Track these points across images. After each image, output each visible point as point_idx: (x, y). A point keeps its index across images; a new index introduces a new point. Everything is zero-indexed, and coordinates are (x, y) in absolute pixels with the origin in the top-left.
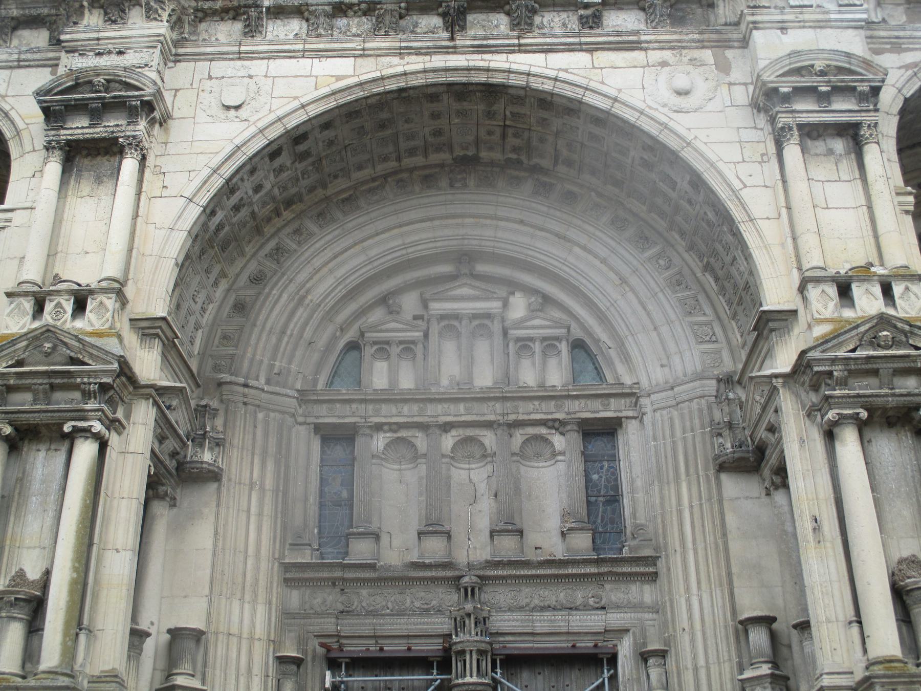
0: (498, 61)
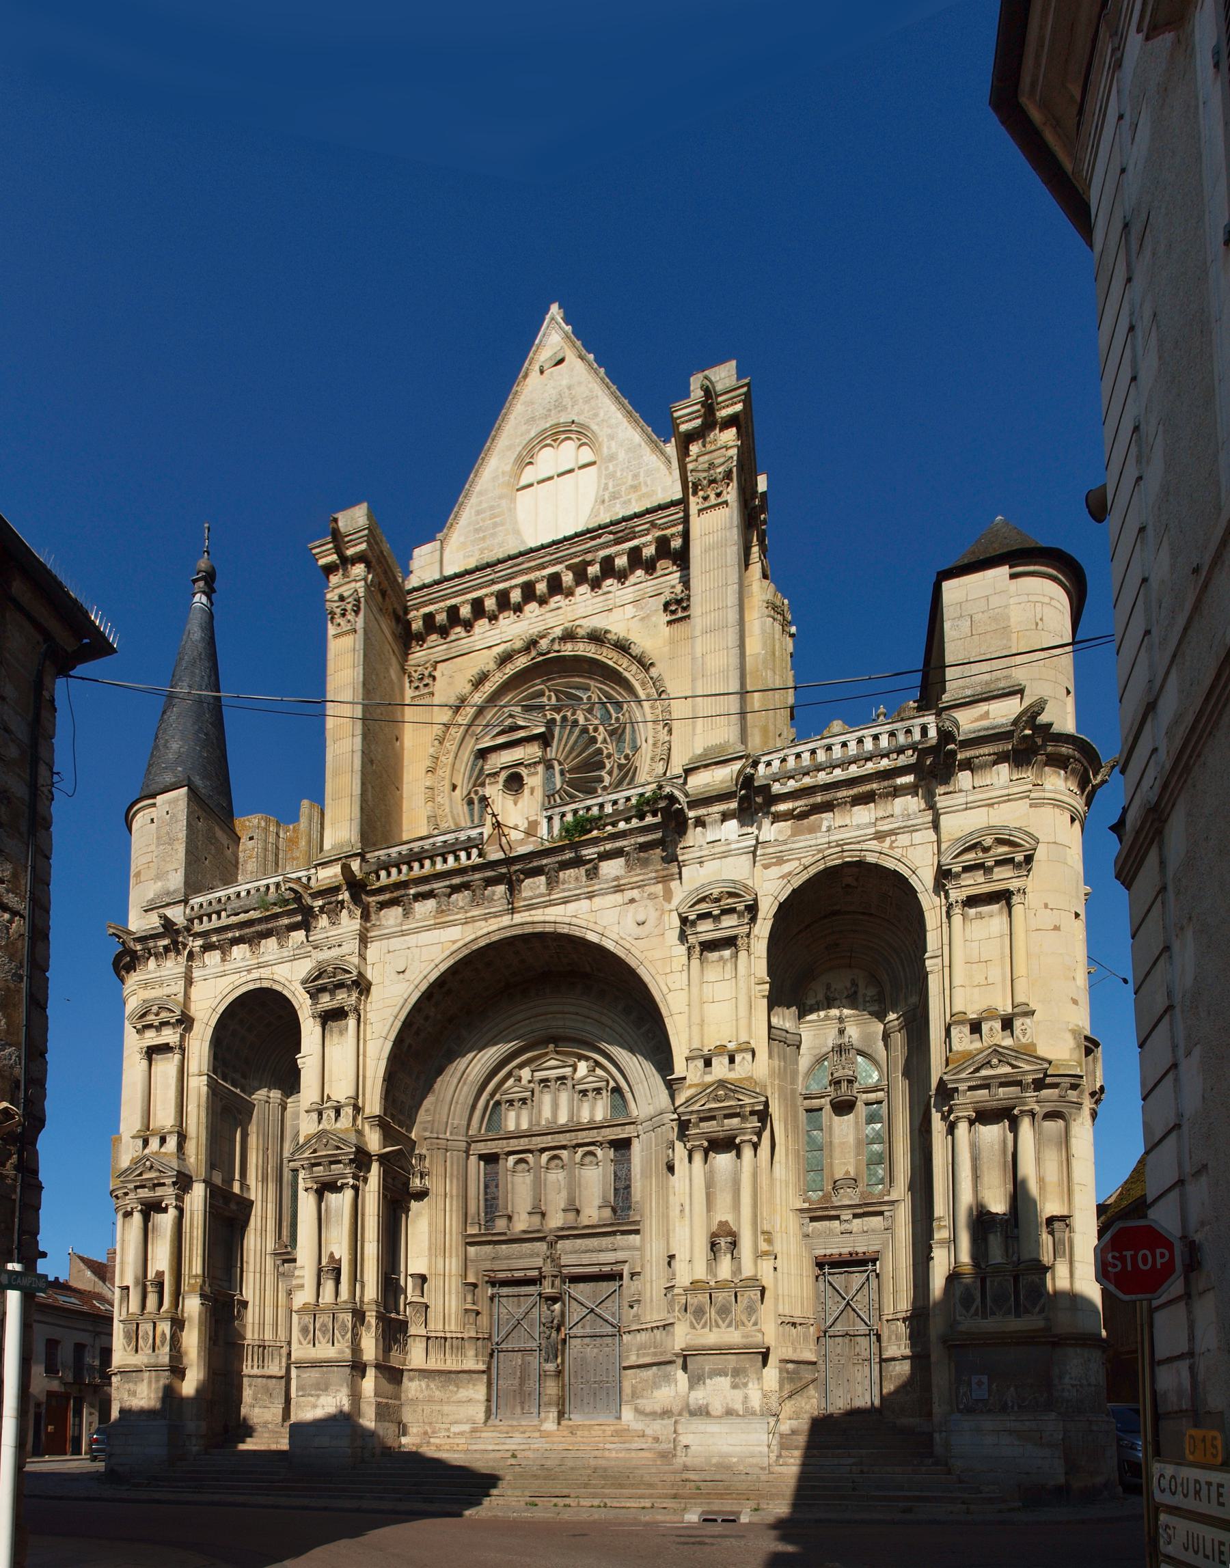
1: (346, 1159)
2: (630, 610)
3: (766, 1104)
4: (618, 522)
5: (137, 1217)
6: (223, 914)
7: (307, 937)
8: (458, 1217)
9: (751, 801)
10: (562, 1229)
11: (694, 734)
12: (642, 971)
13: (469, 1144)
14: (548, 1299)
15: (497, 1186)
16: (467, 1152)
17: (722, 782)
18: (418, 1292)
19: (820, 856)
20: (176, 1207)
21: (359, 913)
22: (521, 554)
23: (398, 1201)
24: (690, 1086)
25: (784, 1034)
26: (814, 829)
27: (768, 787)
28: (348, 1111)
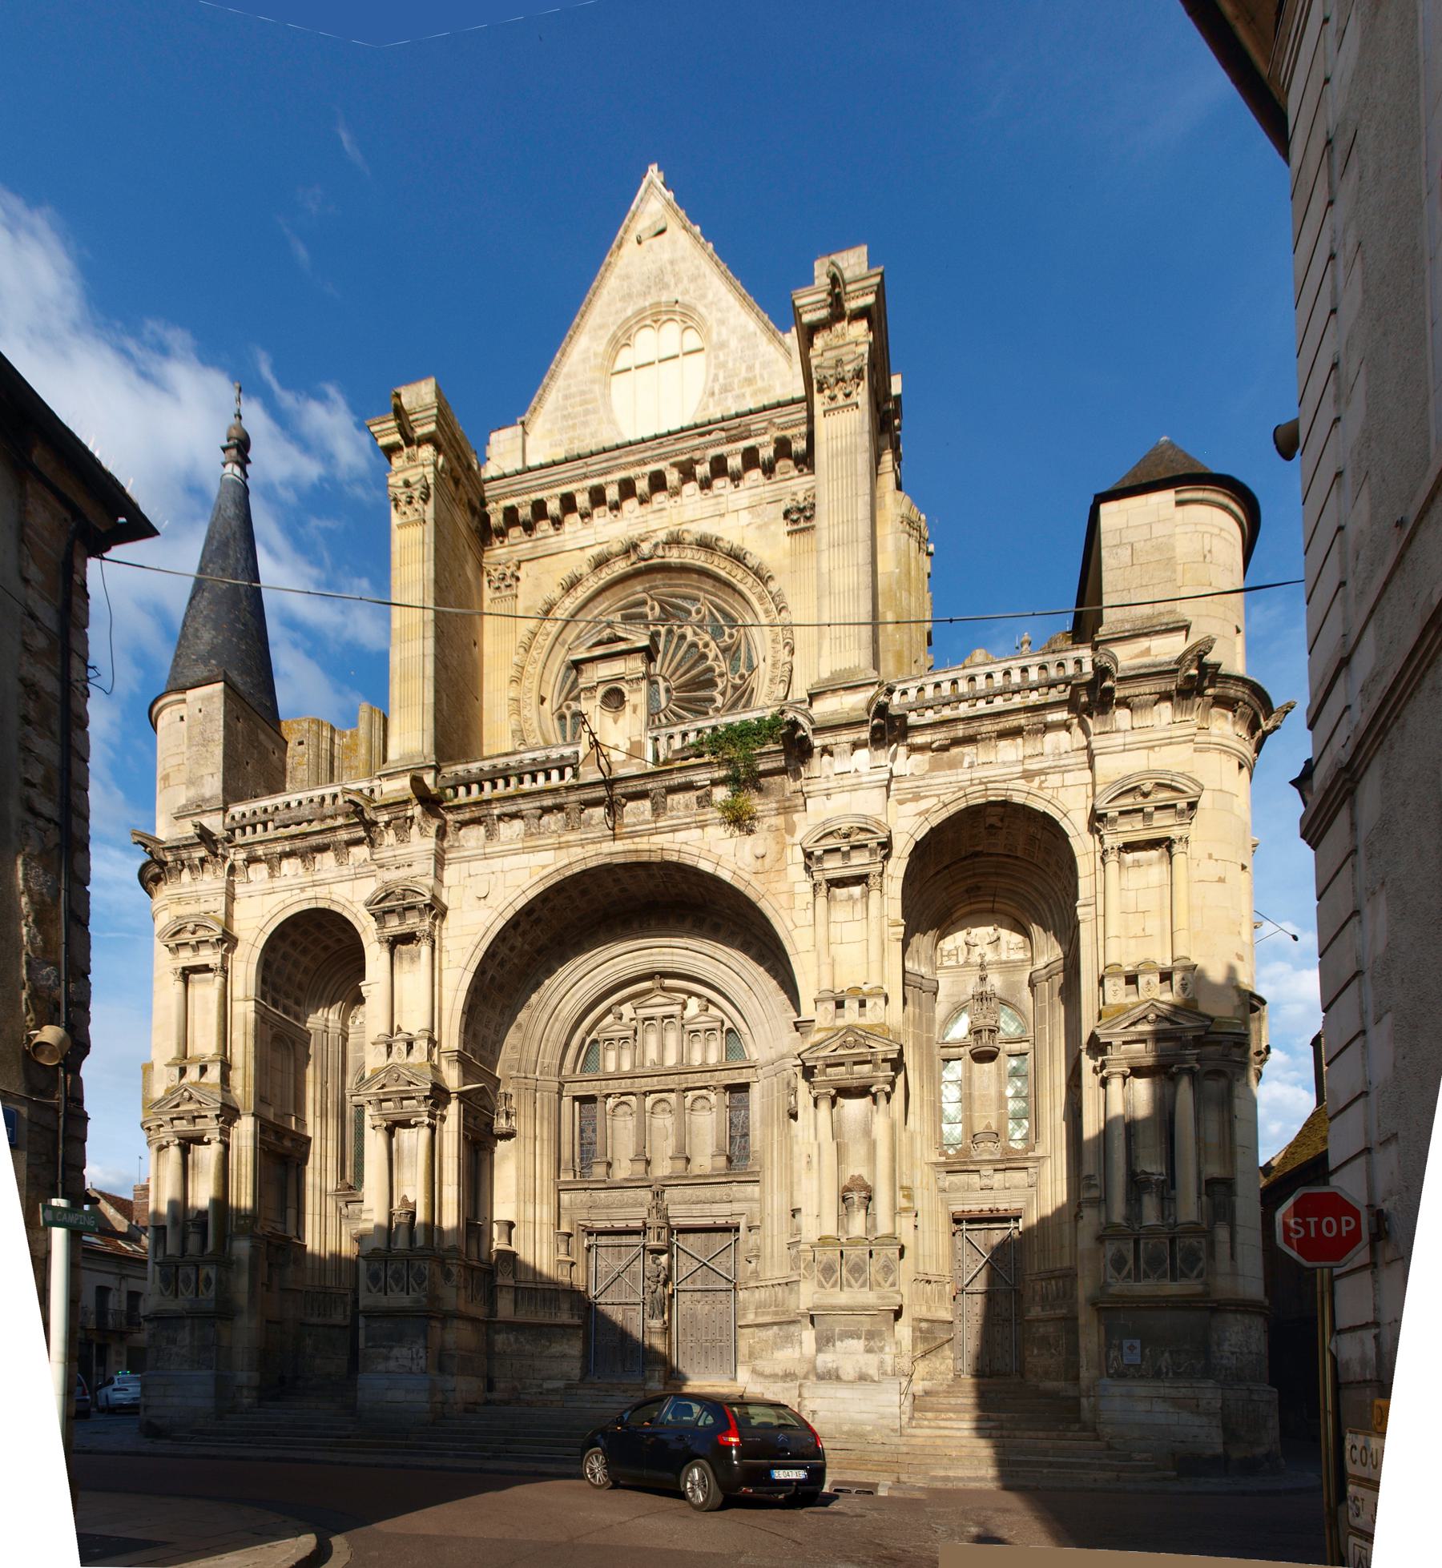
0: (642, 843)
1: (421, 1095)
2: (745, 517)
3: (901, 1052)
4: (731, 418)
5: (174, 1152)
6: (270, 825)
7: (372, 854)
8: (549, 1162)
9: (887, 728)
10: (670, 1178)
11: (819, 656)
12: (763, 905)
13: (561, 1085)
14: (652, 1252)
15: (594, 1131)
16: (560, 1093)
17: (853, 709)
18: (505, 1240)
19: (961, 793)
20: (221, 1141)
21: (432, 831)
22: (618, 447)
23: (479, 1144)
24: (819, 1030)
25: (919, 979)
26: (954, 765)
27: (904, 717)
28: (422, 1045)
